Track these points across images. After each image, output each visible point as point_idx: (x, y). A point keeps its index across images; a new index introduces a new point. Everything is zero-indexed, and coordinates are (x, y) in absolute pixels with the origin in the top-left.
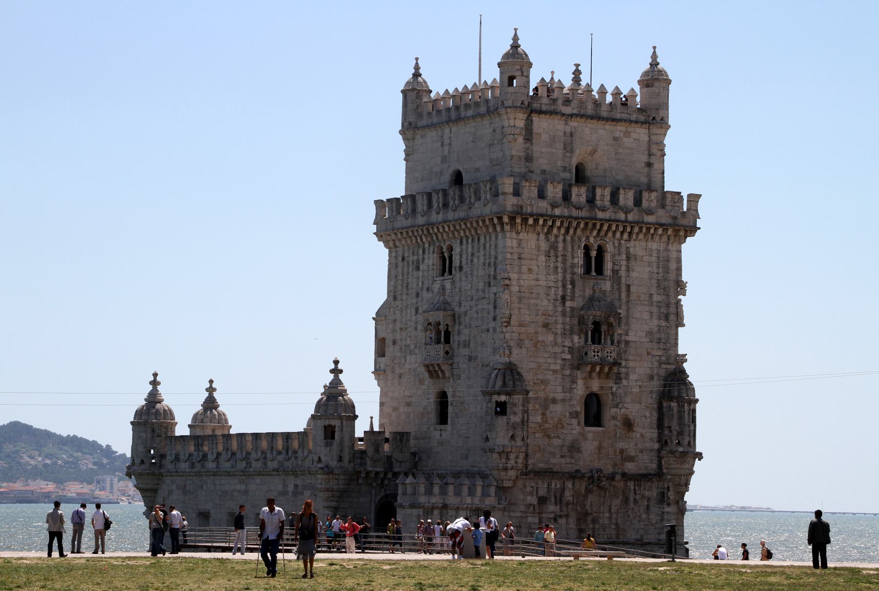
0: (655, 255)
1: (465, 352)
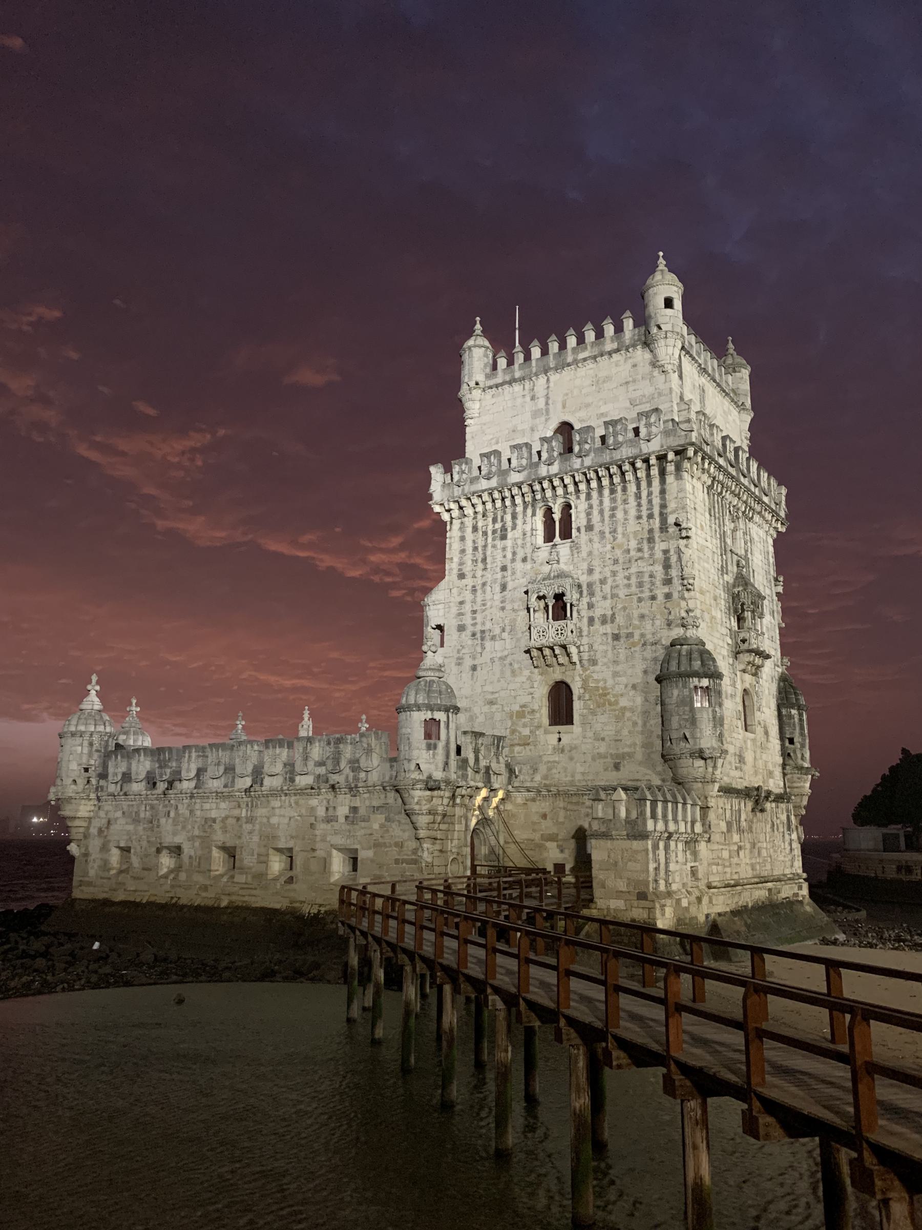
1: (608, 629)
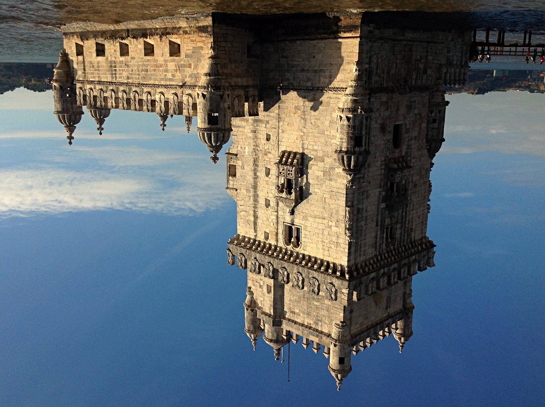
0: (362, 252)
